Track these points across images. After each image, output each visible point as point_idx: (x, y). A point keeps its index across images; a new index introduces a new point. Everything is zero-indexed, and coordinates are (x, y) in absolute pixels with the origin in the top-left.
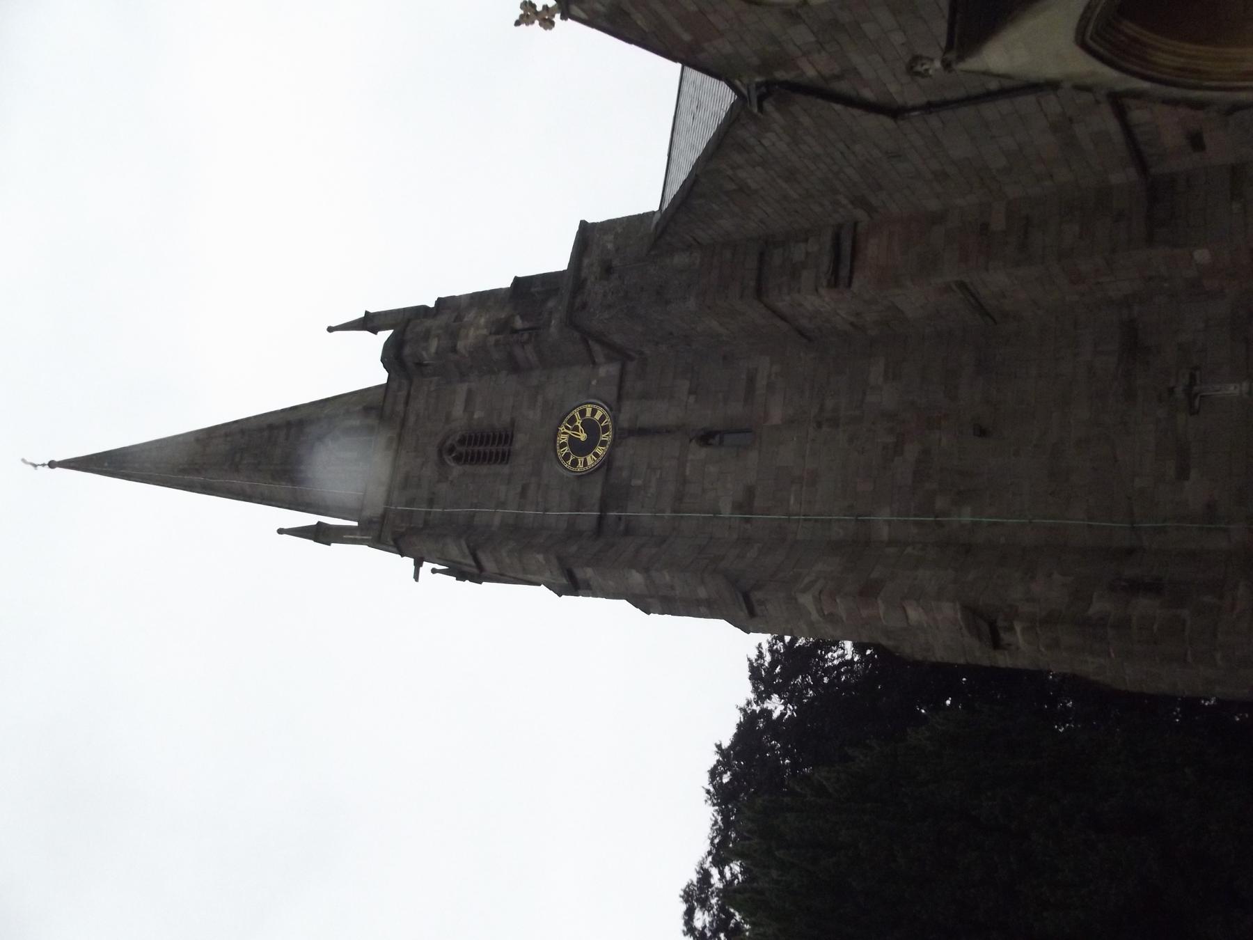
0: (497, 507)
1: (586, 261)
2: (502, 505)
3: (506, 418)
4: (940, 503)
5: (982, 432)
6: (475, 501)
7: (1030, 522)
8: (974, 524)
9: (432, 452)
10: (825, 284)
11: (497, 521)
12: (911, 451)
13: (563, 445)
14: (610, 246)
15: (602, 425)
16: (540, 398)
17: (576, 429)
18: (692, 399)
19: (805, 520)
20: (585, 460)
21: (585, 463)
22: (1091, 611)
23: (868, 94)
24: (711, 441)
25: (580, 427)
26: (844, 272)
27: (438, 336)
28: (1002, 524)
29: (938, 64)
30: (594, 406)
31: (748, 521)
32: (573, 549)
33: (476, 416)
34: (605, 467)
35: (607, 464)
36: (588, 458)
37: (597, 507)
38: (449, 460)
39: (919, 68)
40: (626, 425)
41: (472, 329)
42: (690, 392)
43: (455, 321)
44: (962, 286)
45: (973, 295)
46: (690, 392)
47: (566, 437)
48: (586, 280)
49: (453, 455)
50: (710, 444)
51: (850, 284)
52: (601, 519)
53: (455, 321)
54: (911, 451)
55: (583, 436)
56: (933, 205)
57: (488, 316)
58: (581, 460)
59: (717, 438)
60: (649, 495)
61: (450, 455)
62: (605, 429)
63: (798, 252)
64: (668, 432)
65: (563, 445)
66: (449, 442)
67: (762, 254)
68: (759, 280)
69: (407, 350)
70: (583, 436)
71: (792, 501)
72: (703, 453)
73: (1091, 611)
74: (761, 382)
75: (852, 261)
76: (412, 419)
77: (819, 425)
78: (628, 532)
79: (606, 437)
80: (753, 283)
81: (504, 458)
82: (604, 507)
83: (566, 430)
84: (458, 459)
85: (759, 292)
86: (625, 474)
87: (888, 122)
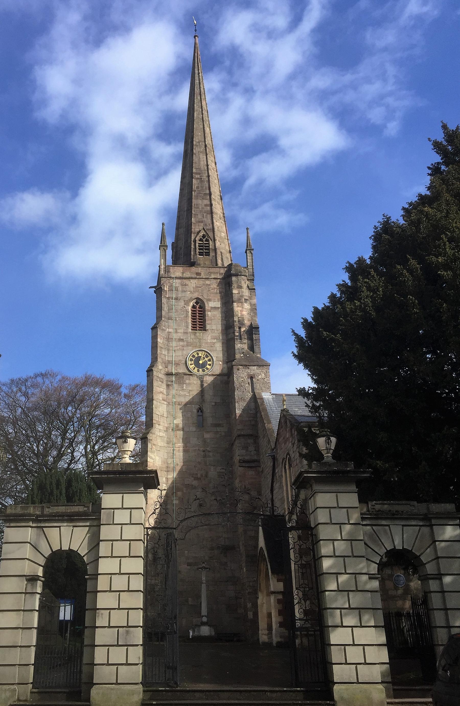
0: (176, 329)
1: (255, 367)
2: (176, 332)
3: (208, 327)
4: (179, 494)
6: (177, 319)
9: (196, 295)
10: (240, 458)
11: (170, 330)
12: (195, 483)
13: (198, 354)
14: (260, 377)
15: (205, 369)
16: (216, 340)
17: (204, 358)
18: (214, 404)
19: (173, 449)
20: (193, 364)
21: (191, 364)
24: (200, 411)
25: (204, 360)
26: (244, 464)
27: (239, 293)
30: (212, 365)
31: (173, 430)
32: (160, 367)
33: (209, 313)
34: (189, 373)
35: (190, 374)
36: (193, 365)
37: (176, 371)
38: (193, 303)
40: (204, 379)
41: (241, 309)
42: (215, 403)
43: (245, 299)
46: (215, 403)
47: (201, 355)
48: (249, 368)
49: (195, 305)
50: (198, 412)
51: (240, 467)
52: (171, 374)
53: (245, 299)
54: (195, 483)
55: (201, 362)
57: (246, 314)
58: (193, 362)
59: (201, 414)
60: (180, 392)
61: (195, 303)
62: (203, 371)
63: (251, 448)
64: (202, 396)
65: (198, 354)
66: (200, 302)
67: (251, 435)
68: (244, 435)
69: (234, 279)
70: (201, 362)
71: (179, 444)
72: (195, 411)
74: (219, 429)
75: (249, 467)
76: (208, 282)
77: (204, 451)
78: (168, 386)
79: (201, 372)
80: (242, 433)
81: (194, 328)
82: (177, 374)
83: (203, 354)
84: (194, 307)
85: (239, 436)
86: (187, 381)
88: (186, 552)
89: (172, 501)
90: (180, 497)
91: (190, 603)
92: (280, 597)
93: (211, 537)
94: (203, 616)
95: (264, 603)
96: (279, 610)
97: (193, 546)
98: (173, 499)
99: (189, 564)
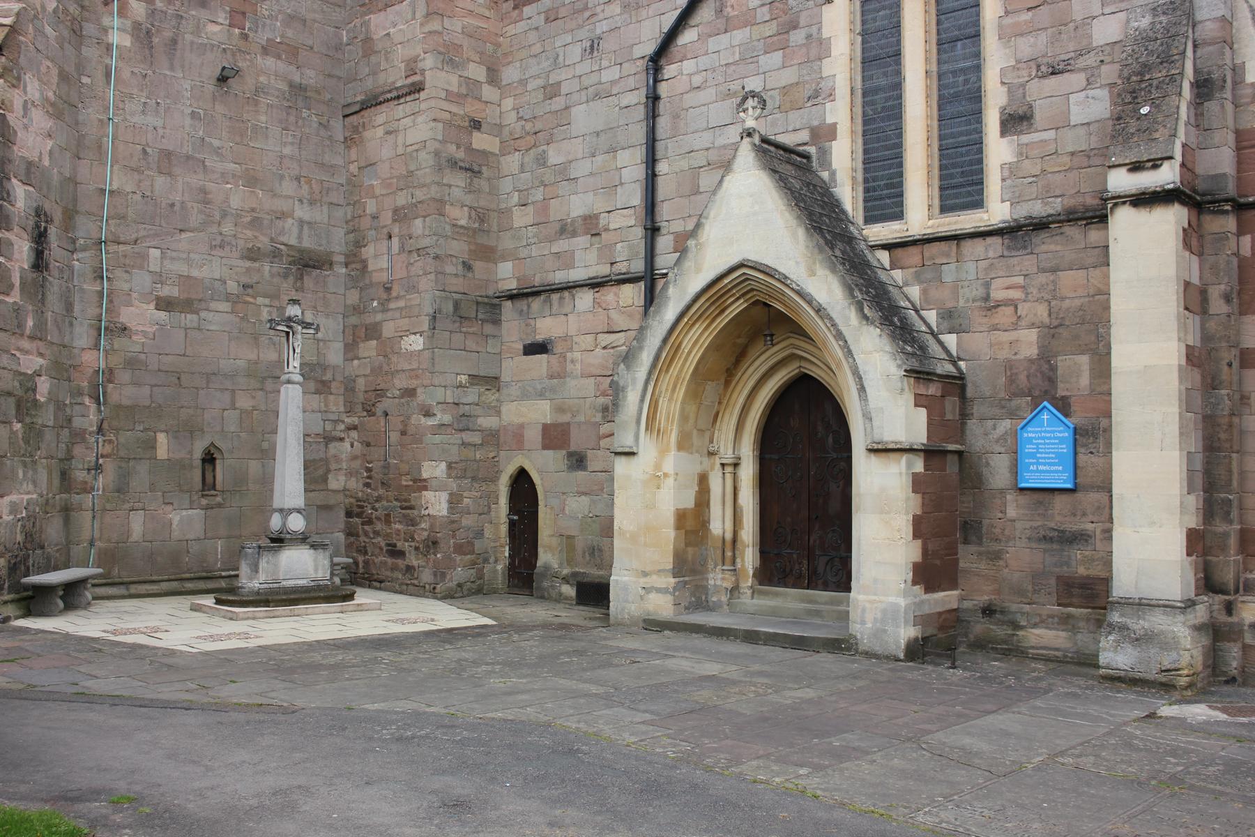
5: (223, 79)
7: (109, 119)
8: (109, 47)
22: (14, 181)
23: (688, 37)
28: (109, 83)
29: (750, 123)
39: (750, 103)
44: (417, 88)
45: (398, 97)
56: (510, 74)
73: (14, 181)
87: (650, 48)
88: (155, 253)
89: (105, 30)
90: (140, 25)
91: (162, 452)
92: (919, 466)
93: (253, 210)
94: (285, 513)
95: (666, 475)
96: (915, 516)
97: (184, 235)
98: (106, 21)
99: (165, 304)
